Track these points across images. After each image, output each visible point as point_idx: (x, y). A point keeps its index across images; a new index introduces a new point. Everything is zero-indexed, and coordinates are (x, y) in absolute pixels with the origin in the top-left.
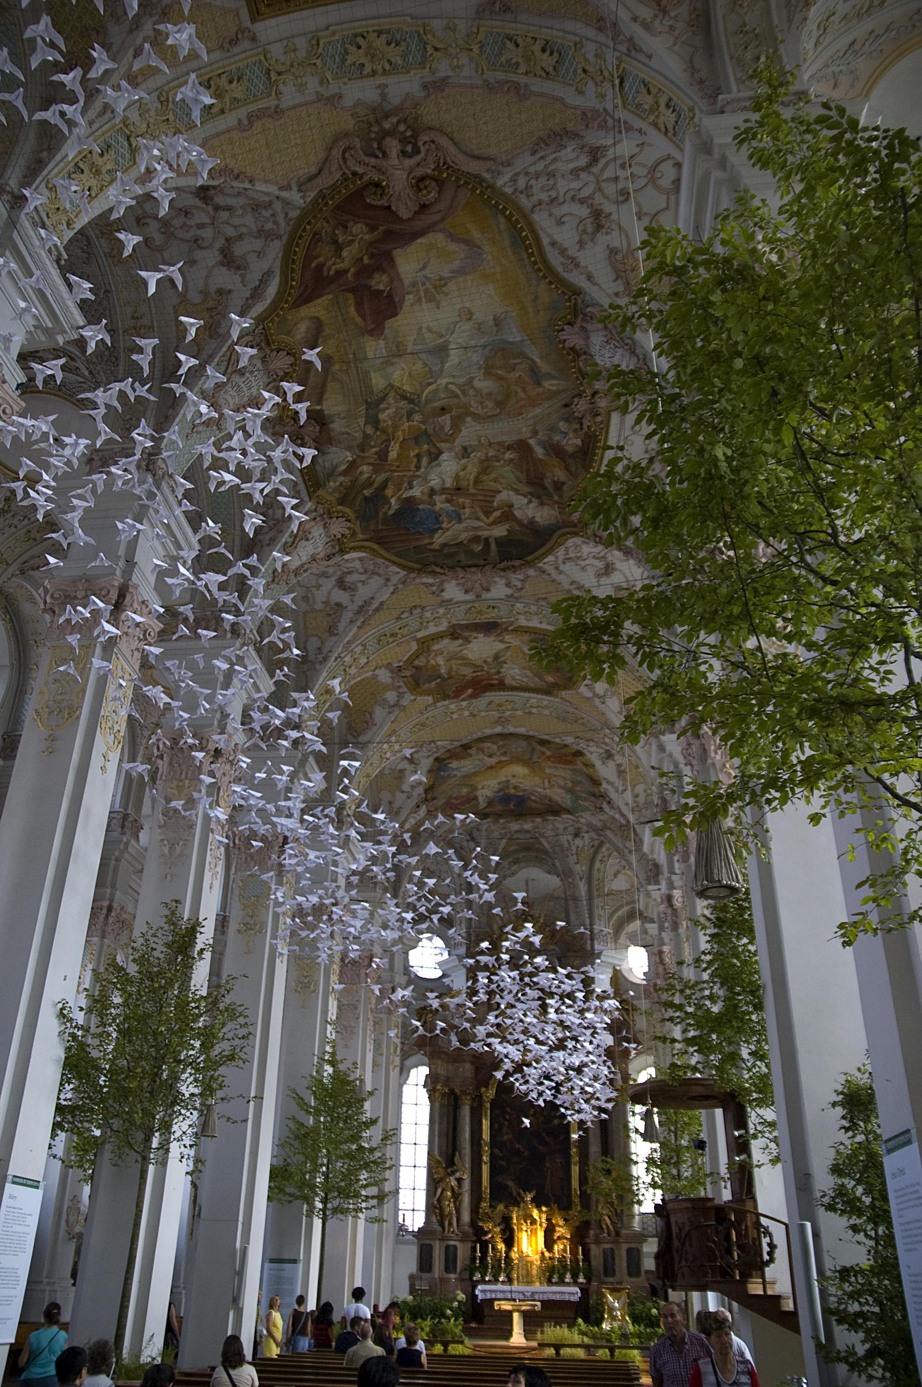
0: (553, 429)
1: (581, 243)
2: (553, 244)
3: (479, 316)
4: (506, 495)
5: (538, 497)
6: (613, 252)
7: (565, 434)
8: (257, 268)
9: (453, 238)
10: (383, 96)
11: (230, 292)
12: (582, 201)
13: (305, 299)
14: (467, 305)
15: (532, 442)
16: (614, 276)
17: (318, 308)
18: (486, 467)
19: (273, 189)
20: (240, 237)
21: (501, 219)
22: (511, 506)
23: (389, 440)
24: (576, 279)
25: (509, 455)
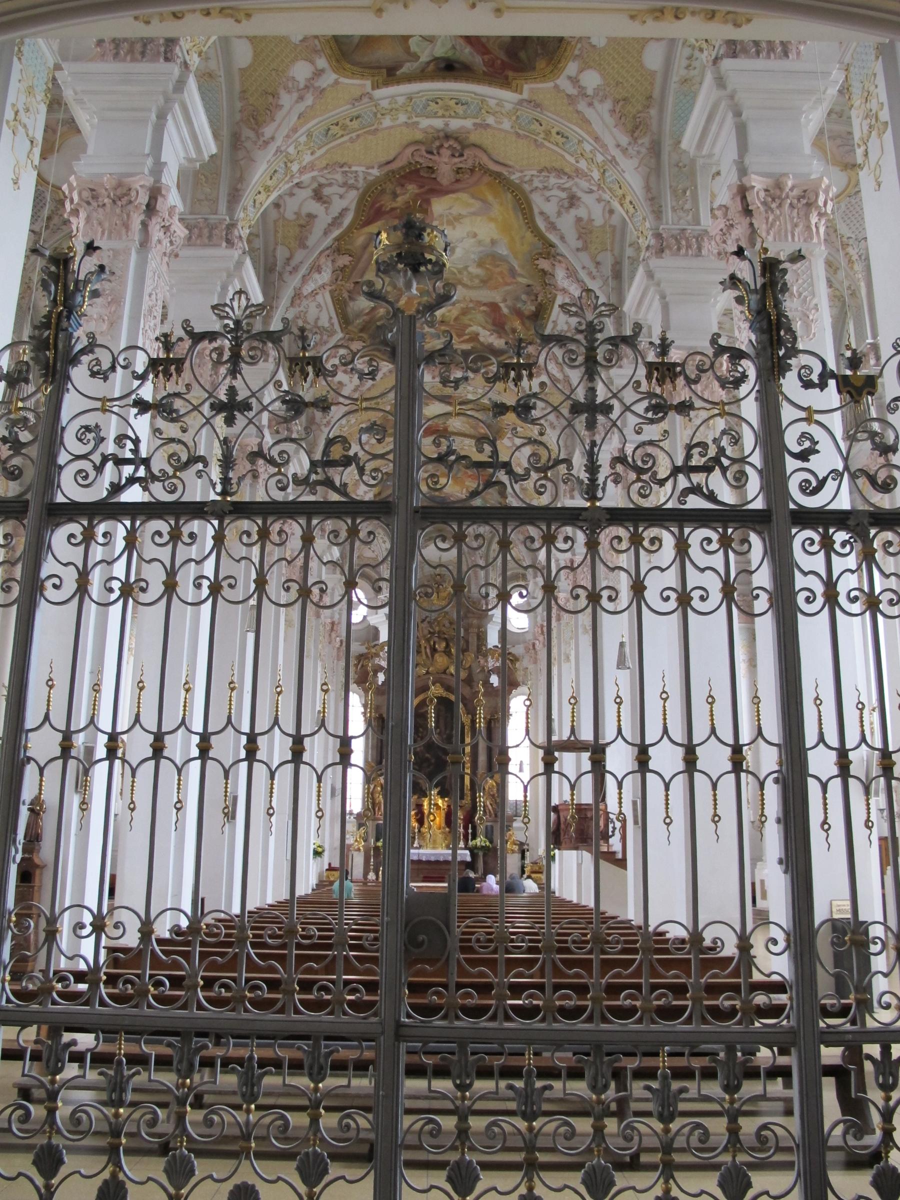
0: (517, 299)
1: (559, 214)
2: (542, 213)
3: (480, 237)
4: (474, 328)
5: (498, 333)
6: (579, 220)
7: (525, 302)
8: (338, 205)
9: (473, 196)
10: (447, 125)
11: (316, 216)
12: (564, 190)
13: (368, 223)
14: (475, 230)
15: (502, 305)
16: (576, 236)
17: (373, 228)
18: (465, 312)
19: (363, 169)
20: (330, 185)
21: (510, 196)
22: (478, 334)
23: (401, 295)
24: (553, 237)
25: (482, 308)
